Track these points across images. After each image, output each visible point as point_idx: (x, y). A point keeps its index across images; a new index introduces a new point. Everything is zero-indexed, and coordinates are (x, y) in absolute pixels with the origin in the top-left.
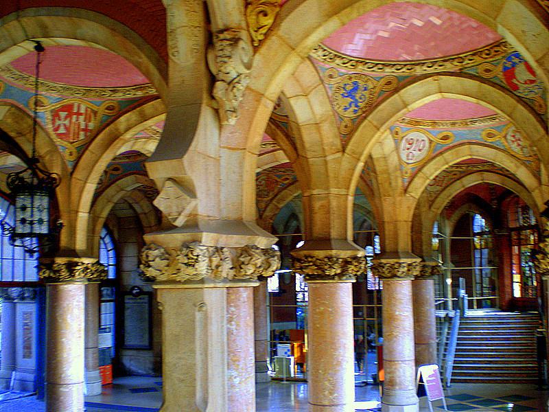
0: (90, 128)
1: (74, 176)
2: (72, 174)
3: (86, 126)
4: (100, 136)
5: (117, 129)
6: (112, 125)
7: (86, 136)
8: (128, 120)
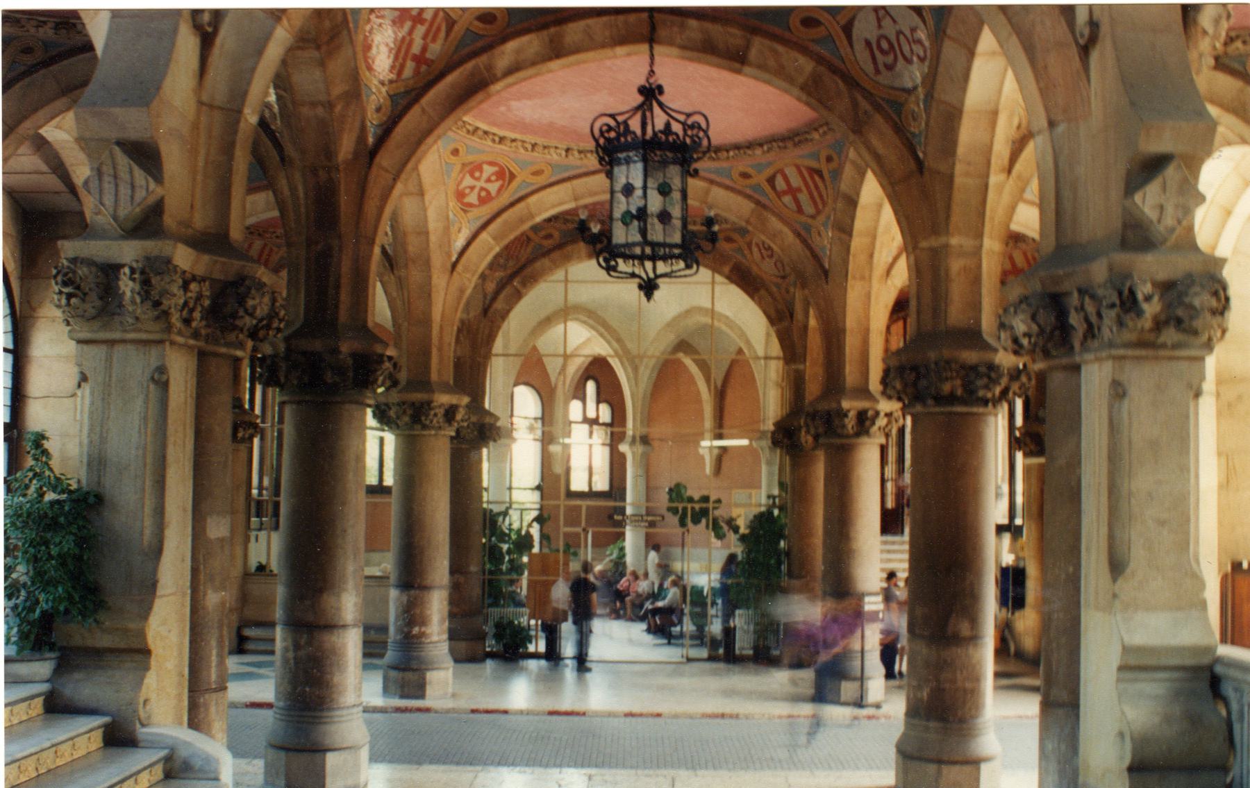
0: (428, 55)
1: (378, 159)
2: (373, 153)
3: (424, 49)
4: (450, 79)
5: (489, 68)
6: (482, 60)
7: (417, 72)
8: (518, 52)
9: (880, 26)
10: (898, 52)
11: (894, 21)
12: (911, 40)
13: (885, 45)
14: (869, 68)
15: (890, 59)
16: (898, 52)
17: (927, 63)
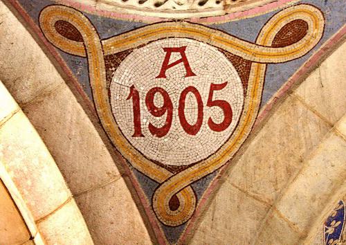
9: (162, 75)
10: (176, 112)
11: (190, 73)
12: (205, 100)
13: (159, 101)
14: (128, 130)
15: (160, 122)
16: (176, 112)
17: (227, 132)
